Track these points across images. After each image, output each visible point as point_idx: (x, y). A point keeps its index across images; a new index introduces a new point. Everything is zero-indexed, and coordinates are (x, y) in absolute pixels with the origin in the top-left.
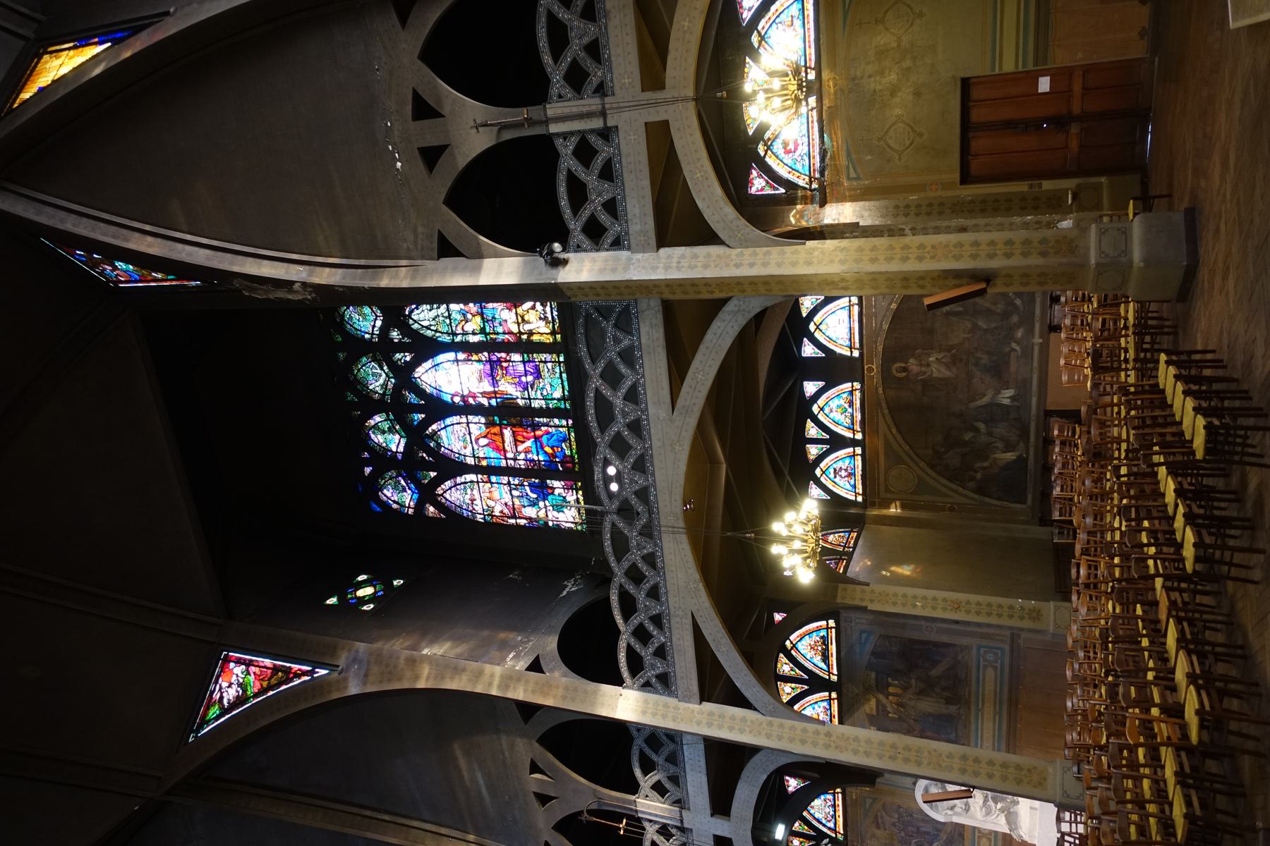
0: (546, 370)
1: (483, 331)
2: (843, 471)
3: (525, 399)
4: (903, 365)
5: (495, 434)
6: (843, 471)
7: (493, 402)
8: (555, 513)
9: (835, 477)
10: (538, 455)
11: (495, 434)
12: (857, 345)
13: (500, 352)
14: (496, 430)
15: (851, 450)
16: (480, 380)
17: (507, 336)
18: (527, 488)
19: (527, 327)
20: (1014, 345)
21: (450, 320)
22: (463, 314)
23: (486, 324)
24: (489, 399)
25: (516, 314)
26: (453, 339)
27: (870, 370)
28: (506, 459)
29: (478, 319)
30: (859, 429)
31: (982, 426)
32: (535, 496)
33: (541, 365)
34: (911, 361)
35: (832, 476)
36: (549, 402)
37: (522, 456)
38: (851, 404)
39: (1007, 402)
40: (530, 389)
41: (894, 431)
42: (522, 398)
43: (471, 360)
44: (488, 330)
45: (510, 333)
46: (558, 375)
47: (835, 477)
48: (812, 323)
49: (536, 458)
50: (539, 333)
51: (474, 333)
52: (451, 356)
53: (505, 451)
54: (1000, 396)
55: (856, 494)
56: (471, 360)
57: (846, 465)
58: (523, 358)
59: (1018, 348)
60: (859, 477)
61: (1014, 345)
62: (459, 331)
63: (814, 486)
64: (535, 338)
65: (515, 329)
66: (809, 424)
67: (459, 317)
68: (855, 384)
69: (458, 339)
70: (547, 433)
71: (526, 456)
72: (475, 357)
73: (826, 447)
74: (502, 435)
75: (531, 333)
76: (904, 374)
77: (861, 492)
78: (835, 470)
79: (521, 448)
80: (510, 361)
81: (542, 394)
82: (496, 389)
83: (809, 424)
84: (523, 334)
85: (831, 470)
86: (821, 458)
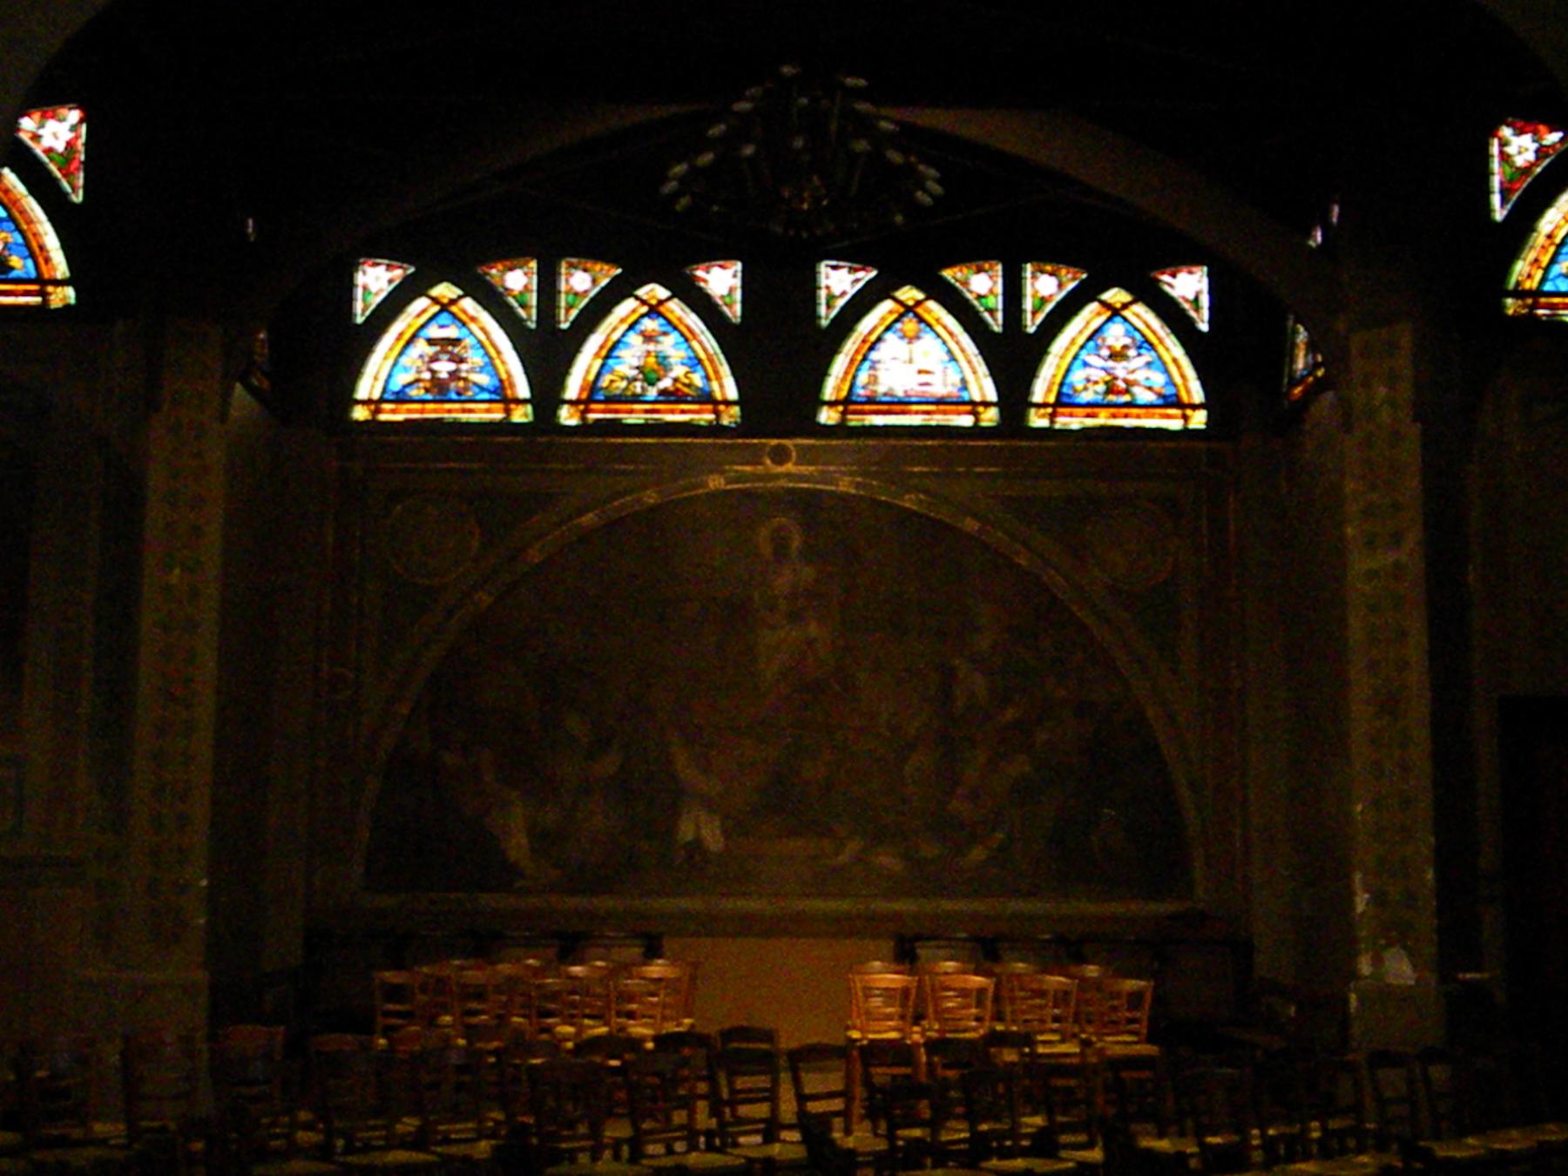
2: (452, 366)
4: (796, 542)
6: (452, 366)
9: (431, 342)
12: (854, 421)
15: (523, 390)
20: (854, 846)
27: (780, 456)
30: (592, 416)
31: (609, 765)
34: (808, 573)
35: (434, 332)
38: (673, 397)
39: (686, 831)
41: (589, 519)
47: (431, 342)
48: (920, 296)
54: (703, 816)
55: (375, 404)
57: (474, 377)
59: (843, 859)
60: (432, 412)
61: (854, 846)
63: (398, 274)
66: (608, 273)
68: (736, 410)
73: (530, 317)
76: (767, 550)
77: (383, 417)
78: (456, 342)
83: (608, 273)
85: (452, 332)
86: (494, 301)
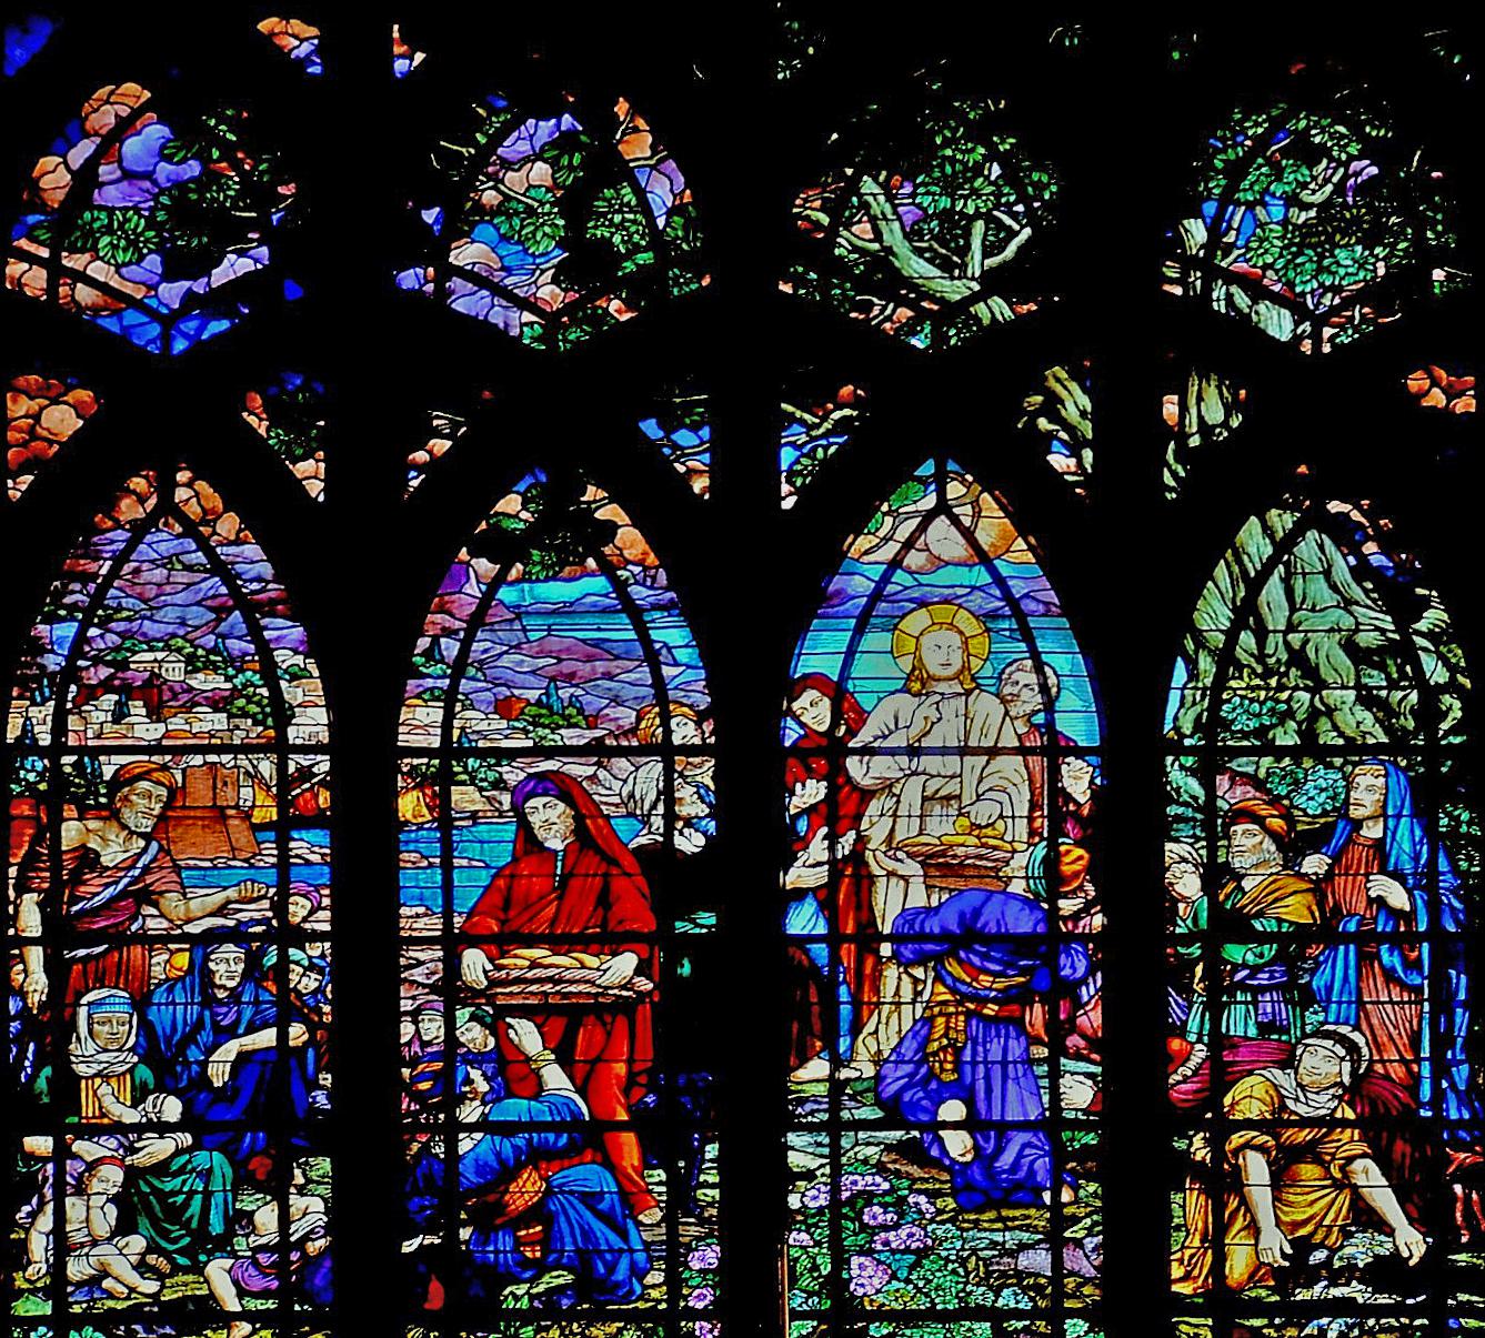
0: (1010, 1239)
1: (1230, 924)
3: (835, 1106)
5: (604, 900)
7: (803, 920)
8: (111, 1178)
10: (483, 1125)
11: (604, 900)
13: (1107, 997)
14: (636, 911)
16: (938, 864)
17: (1200, 1053)
18: (267, 1038)
19: (1257, 1169)
21: (1295, 753)
22: (1329, 830)
23: (1269, 951)
24: (826, 899)
25: (1331, 1123)
26: (1178, 749)
28: (452, 944)
29: (1297, 909)
32: (219, 1073)
33: (1040, 1218)
36: (823, 1233)
37: (474, 1036)
40: (895, 1135)
42: (837, 1087)
43: (1057, 830)
44: (1235, 952)
45: (1220, 1075)
46: (980, 1295)
49: (470, 1112)
50: (1221, 1228)
51: (1215, 875)
52: (1079, 721)
53: (498, 945)
56: (1057, 830)
58: (1075, 1125)
62: (1230, 795)
64: (1190, 1206)
65: (1249, 1097)
67: (1312, 803)
69: (1181, 779)
70: (632, 1200)
71: (476, 1059)
72: (1074, 857)
74: (611, 943)
75: (1223, 1183)
79: (527, 1036)
80: (1058, 1050)
81: (868, 1197)
82: (886, 949)
84: (1216, 1143)
